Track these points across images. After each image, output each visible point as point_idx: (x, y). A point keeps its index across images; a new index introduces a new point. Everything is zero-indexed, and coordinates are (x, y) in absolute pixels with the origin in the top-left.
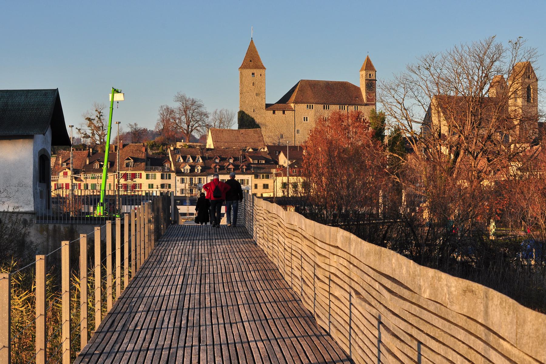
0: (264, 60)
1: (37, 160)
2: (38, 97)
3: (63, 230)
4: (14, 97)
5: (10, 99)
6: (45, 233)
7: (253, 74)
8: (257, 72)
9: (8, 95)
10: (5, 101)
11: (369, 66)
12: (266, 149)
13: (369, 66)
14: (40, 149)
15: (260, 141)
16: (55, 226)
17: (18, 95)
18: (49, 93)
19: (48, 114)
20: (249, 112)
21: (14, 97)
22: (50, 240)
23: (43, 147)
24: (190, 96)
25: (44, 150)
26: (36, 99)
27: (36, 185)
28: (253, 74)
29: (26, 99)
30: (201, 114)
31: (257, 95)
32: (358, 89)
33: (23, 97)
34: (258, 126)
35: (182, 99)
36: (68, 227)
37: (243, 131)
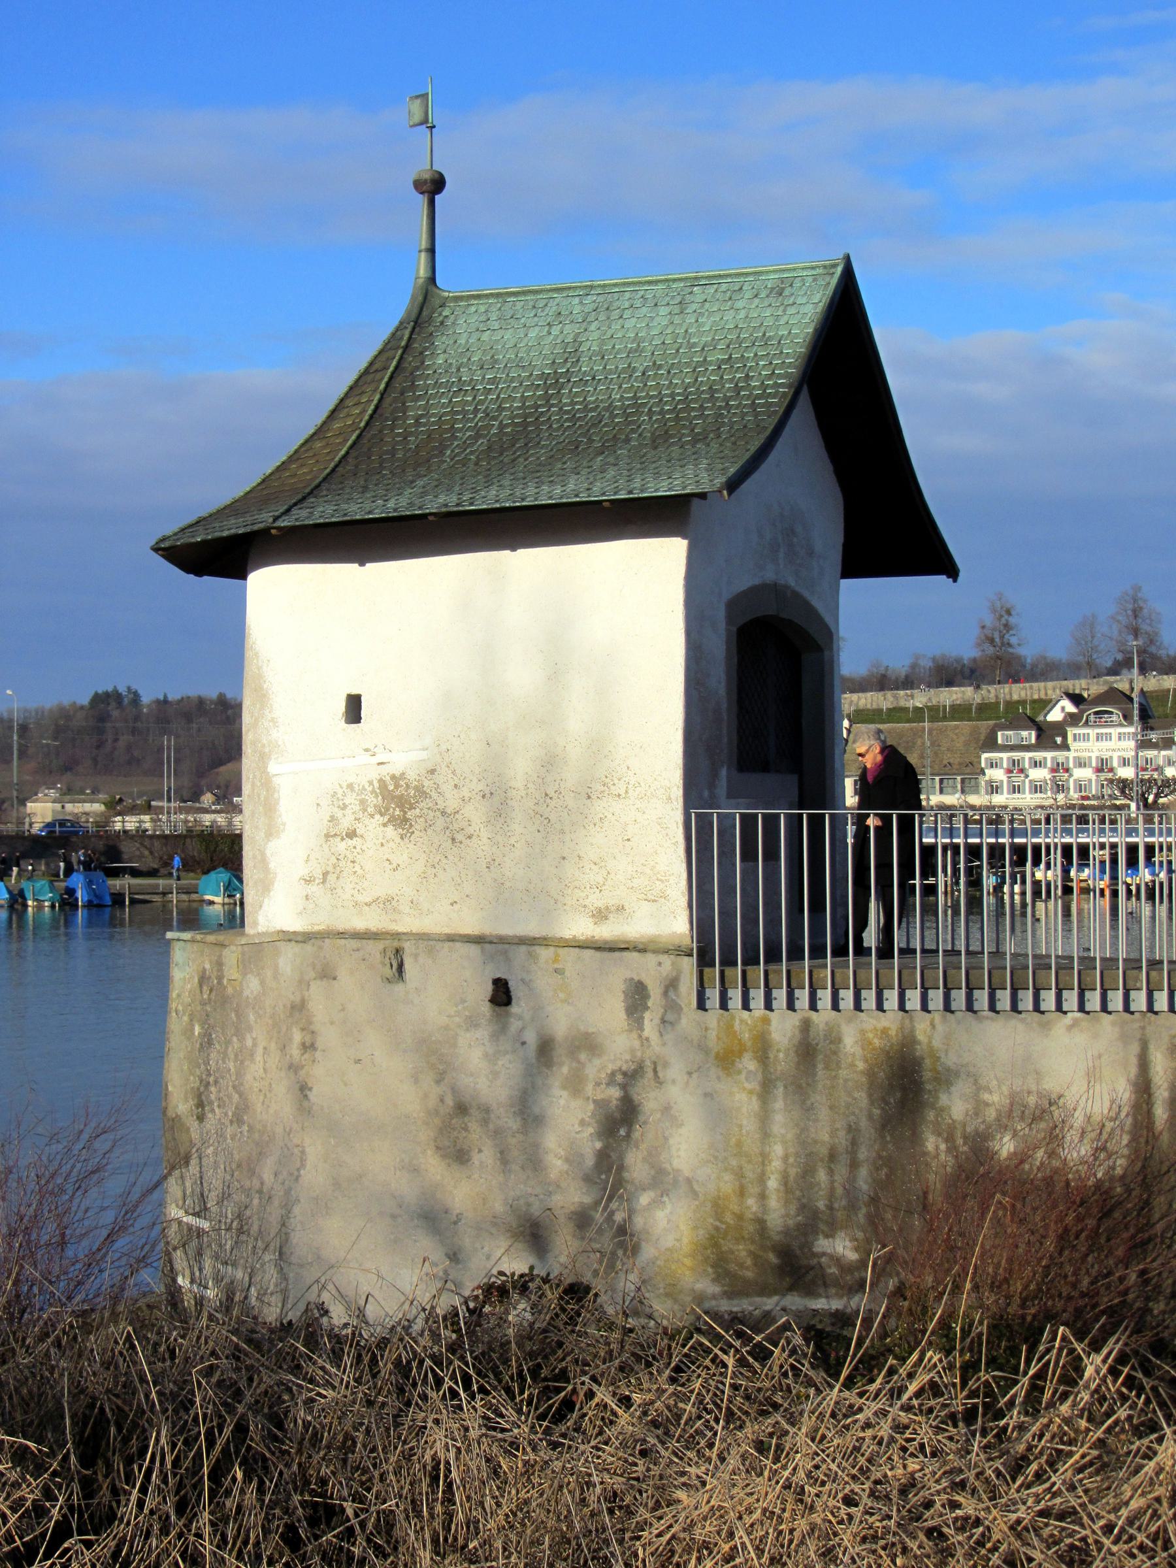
1: (718, 645)
2: (740, 304)
3: (858, 1051)
5: (593, 327)
6: (749, 1063)
9: (593, 306)
10: (569, 339)
14: (744, 582)
16: (806, 1025)
17: (638, 304)
18: (797, 284)
19: (776, 385)
22: (779, 1104)
25: (775, 590)
26: (729, 316)
27: (712, 786)
29: (677, 320)
33: (663, 311)
36: (885, 1031)
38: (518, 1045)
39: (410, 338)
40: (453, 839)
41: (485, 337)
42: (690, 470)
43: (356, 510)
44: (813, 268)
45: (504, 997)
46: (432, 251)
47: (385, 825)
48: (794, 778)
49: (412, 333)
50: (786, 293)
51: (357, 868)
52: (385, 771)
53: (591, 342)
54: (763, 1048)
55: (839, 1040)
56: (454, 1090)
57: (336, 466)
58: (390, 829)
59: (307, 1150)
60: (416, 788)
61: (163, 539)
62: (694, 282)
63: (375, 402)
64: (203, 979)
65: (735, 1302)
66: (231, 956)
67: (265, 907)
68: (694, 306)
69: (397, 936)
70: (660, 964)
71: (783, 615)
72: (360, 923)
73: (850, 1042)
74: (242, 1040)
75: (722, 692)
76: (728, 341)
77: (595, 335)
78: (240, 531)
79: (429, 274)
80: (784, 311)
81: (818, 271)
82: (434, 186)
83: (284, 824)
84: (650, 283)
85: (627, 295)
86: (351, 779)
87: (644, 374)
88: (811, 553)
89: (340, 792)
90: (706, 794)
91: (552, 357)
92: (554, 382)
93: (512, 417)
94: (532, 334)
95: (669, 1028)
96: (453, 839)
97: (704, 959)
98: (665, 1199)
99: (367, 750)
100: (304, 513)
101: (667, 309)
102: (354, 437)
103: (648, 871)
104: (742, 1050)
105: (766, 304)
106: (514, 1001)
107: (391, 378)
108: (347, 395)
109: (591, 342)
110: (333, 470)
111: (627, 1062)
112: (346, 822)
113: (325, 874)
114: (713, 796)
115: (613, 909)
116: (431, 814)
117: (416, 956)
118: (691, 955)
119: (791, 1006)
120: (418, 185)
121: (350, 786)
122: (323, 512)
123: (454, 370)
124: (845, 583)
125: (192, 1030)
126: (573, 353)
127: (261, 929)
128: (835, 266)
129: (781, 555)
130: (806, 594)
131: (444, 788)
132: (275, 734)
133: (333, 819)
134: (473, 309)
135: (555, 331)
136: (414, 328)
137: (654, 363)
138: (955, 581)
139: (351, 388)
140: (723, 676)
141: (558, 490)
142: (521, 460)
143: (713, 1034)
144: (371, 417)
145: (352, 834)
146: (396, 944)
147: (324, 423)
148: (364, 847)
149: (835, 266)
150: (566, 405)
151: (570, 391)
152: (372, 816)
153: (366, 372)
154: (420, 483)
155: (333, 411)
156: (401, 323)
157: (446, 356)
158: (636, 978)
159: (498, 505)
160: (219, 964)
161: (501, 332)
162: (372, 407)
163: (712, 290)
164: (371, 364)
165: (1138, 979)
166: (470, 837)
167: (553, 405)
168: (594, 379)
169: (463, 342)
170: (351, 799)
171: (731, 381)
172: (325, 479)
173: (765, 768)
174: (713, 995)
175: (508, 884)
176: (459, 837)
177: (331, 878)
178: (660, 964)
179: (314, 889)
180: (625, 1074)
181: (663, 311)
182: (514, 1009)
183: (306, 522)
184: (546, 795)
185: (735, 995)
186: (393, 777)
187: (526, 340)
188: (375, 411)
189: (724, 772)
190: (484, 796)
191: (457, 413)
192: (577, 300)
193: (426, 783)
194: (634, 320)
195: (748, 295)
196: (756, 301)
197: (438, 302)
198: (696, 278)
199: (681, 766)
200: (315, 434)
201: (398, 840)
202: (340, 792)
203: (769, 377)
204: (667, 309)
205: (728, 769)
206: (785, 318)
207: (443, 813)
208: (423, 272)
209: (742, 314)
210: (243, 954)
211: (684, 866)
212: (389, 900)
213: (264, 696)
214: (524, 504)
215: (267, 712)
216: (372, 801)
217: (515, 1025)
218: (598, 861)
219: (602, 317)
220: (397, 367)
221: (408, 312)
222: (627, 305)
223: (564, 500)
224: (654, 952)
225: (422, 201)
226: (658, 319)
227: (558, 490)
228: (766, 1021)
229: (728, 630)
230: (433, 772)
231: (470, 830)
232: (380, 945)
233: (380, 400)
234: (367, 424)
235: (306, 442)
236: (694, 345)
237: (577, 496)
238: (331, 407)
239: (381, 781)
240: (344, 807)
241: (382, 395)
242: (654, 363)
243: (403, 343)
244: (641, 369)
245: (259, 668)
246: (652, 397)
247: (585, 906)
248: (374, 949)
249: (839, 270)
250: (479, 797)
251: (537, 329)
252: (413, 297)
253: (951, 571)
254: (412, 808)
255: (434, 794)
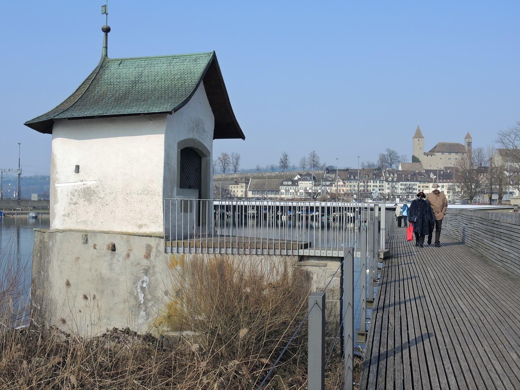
0: (424, 134)
2: (185, 63)
4: (153, 65)
6: (179, 268)
7: (419, 140)
8: (420, 139)
10: (140, 71)
11: (468, 136)
12: (424, 171)
13: (468, 136)
14: (183, 138)
15: (421, 168)
16: (195, 257)
18: (201, 58)
20: (417, 155)
21: (153, 65)
23: (191, 136)
24: (392, 149)
26: (182, 66)
27: (172, 192)
28: (419, 140)
29: (168, 67)
30: (396, 157)
31: (420, 149)
32: (464, 146)
34: (420, 162)
35: (388, 150)
37: (414, 163)
38: (117, 261)
39: (99, 71)
40: (102, 205)
41: (118, 70)
42: (165, 106)
43: (76, 115)
44: (205, 54)
45: (114, 248)
46: (106, 48)
47: (84, 201)
48: (198, 190)
49: (100, 69)
50: (197, 60)
51: (77, 212)
52: (85, 186)
53: (146, 72)
54: (183, 262)
55: (203, 261)
56: (100, 273)
57: (75, 103)
58: (86, 203)
59: (61, 289)
60: (93, 191)
61: (27, 122)
62: (174, 57)
63: (88, 87)
64: (41, 241)
65: (174, 333)
66: (46, 236)
67: (53, 223)
68: (173, 64)
69: (86, 231)
70: (155, 240)
71: (195, 147)
72: (77, 228)
73: (206, 261)
74: (48, 258)
75: (176, 167)
76: (181, 73)
77: (147, 71)
78: (45, 120)
79: (106, 54)
80: (196, 65)
81: (206, 55)
82: (107, 30)
83: (59, 200)
84: (162, 57)
85: (156, 60)
86: (76, 188)
87: (158, 81)
88: (204, 131)
89: (73, 191)
90: (170, 194)
91: (135, 76)
92: (135, 83)
93: (122, 92)
94: (131, 70)
95: (157, 257)
96: (102, 205)
97: (167, 238)
98: (155, 304)
99: (80, 180)
100: (62, 115)
101: (166, 64)
102: (81, 96)
103: (153, 215)
104: (177, 263)
105: (192, 63)
106: (116, 250)
107: (93, 81)
108: (81, 85)
109: (146, 72)
110: (74, 104)
111: (146, 266)
112: (75, 200)
113: (69, 214)
114: (172, 195)
115: (144, 225)
116: (97, 198)
117: (91, 237)
118: (163, 238)
119: (190, 253)
120: (103, 30)
121: (76, 190)
122: (68, 115)
123: (109, 79)
124: (216, 141)
125: (38, 255)
126: (141, 75)
127: (53, 228)
128: (211, 54)
129: (195, 131)
130: (202, 142)
131: (100, 191)
132: (57, 176)
133: (71, 199)
134: (116, 63)
135: (137, 69)
136: (100, 68)
137: (161, 78)
138: (244, 140)
139: (83, 83)
140: (176, 163)
141: (130, 110)
142: (123, 102)
143: (169, 259)
144: (86, 91)
145: (75, 204)
146: (86, 233)
147: (75, 92)
148: (79, 207)
149: (211, 54)
150: (137, 89)
151: (139, 85)
152: (81, 198)
153: (87, 79)
154: (95, 108)
155: (78, 89)
156: (97, 67)
157: (108, 75)
158: (149, 244)
159: (113, 114)
160: (44, 238)
161: (123, 69)
162: (87, 88)
163: (178, 59)
164: (89, 77)
165: (284, 246)
166: (107, 205)
167: (133, 89)
168: (145, 82)
169: (112, 72)
170: (76, 194)
171: (180, 83)
172: (71, 107)
173: (190, 187)
174: (169, 249)
175: (116, 218)
176: (104, 205)
177: (70, 215)
178: (155, 240)
179: (66, 218)
180: (145, 270)
181: (165, 65)
182: (116, 251)
183: (62, 117)
184: (127, 193)
185: (175, 249)
186: (87, 188)
187: (129, 72)
188: (87, 89)
189: (176, 188)
190: (111, 194)
191: (108, 90)
192: (143, 61)
193: (96, 190)
194: (157, 67)
195: (188, 61)
196: (190, 62)
197: (107, 61)
198: (175, 56)
199: (162, 185)
200: (72, 95)
201: (88, 205)
202: (73, 191)
203: (190, 82)
204: (166, 64)
205: (177, 187)
206: (197, 67)
207: (100, 198)
208: (104, 54)
209: (185, 66)
210: (49, 235)
211: (163, 213)
212: (85, 221)
213: (54, 165)
214: (120, 114)
215: (55, 170)
216: (82, 194)
217: (117, 256)
218: (140, 212)
219: (149, 66)
220: (94, 78)
221: (100, 63)
222: (156, 63)
223: (130, 113)
224: (154, 237)
225: (103, 34)
226: (164, 67)
227: (130, 110)
228: (183, 256)
229: (178, 150)
230: (97, 187)
231: (107, 203)
232: (82, 233)
233: (89, 87)
234: (85, 93)
235: (70, 97)
236: (172, 74)
237: (134, 112)
238: (77, 88)
239: (84, 189)
240: (74, 196)
241: (90, 85)
242: (161, 78)
243: (97, 72)
244: (158, 80)
245: (54, 158)
246: (159, 87)
247: (136, 224)
248: (80, 234)
249: (212, 55)
250: (109, 194)
251: (132, 69)
252: (101, 60)
253: (243, 138)
254: (92, 196)
255: (98, 193)
